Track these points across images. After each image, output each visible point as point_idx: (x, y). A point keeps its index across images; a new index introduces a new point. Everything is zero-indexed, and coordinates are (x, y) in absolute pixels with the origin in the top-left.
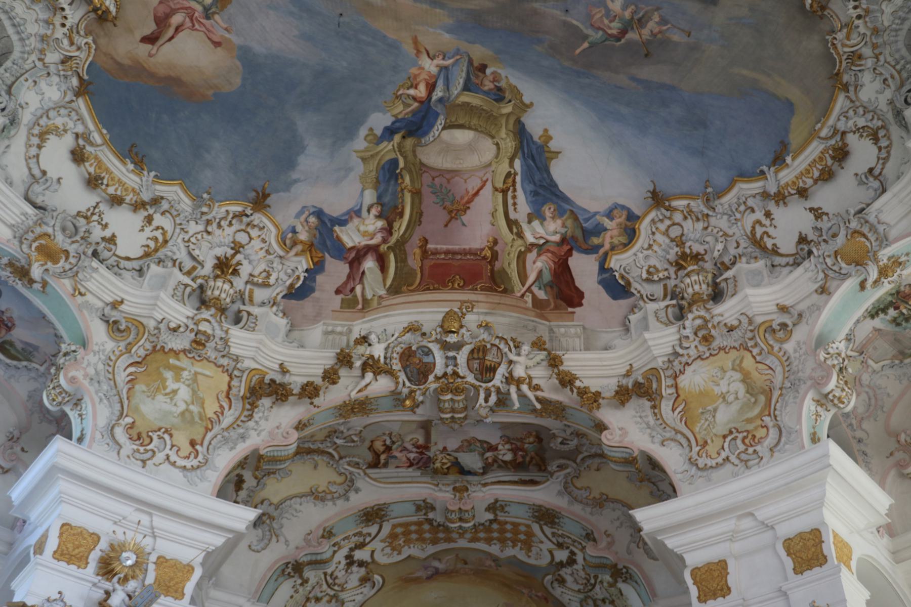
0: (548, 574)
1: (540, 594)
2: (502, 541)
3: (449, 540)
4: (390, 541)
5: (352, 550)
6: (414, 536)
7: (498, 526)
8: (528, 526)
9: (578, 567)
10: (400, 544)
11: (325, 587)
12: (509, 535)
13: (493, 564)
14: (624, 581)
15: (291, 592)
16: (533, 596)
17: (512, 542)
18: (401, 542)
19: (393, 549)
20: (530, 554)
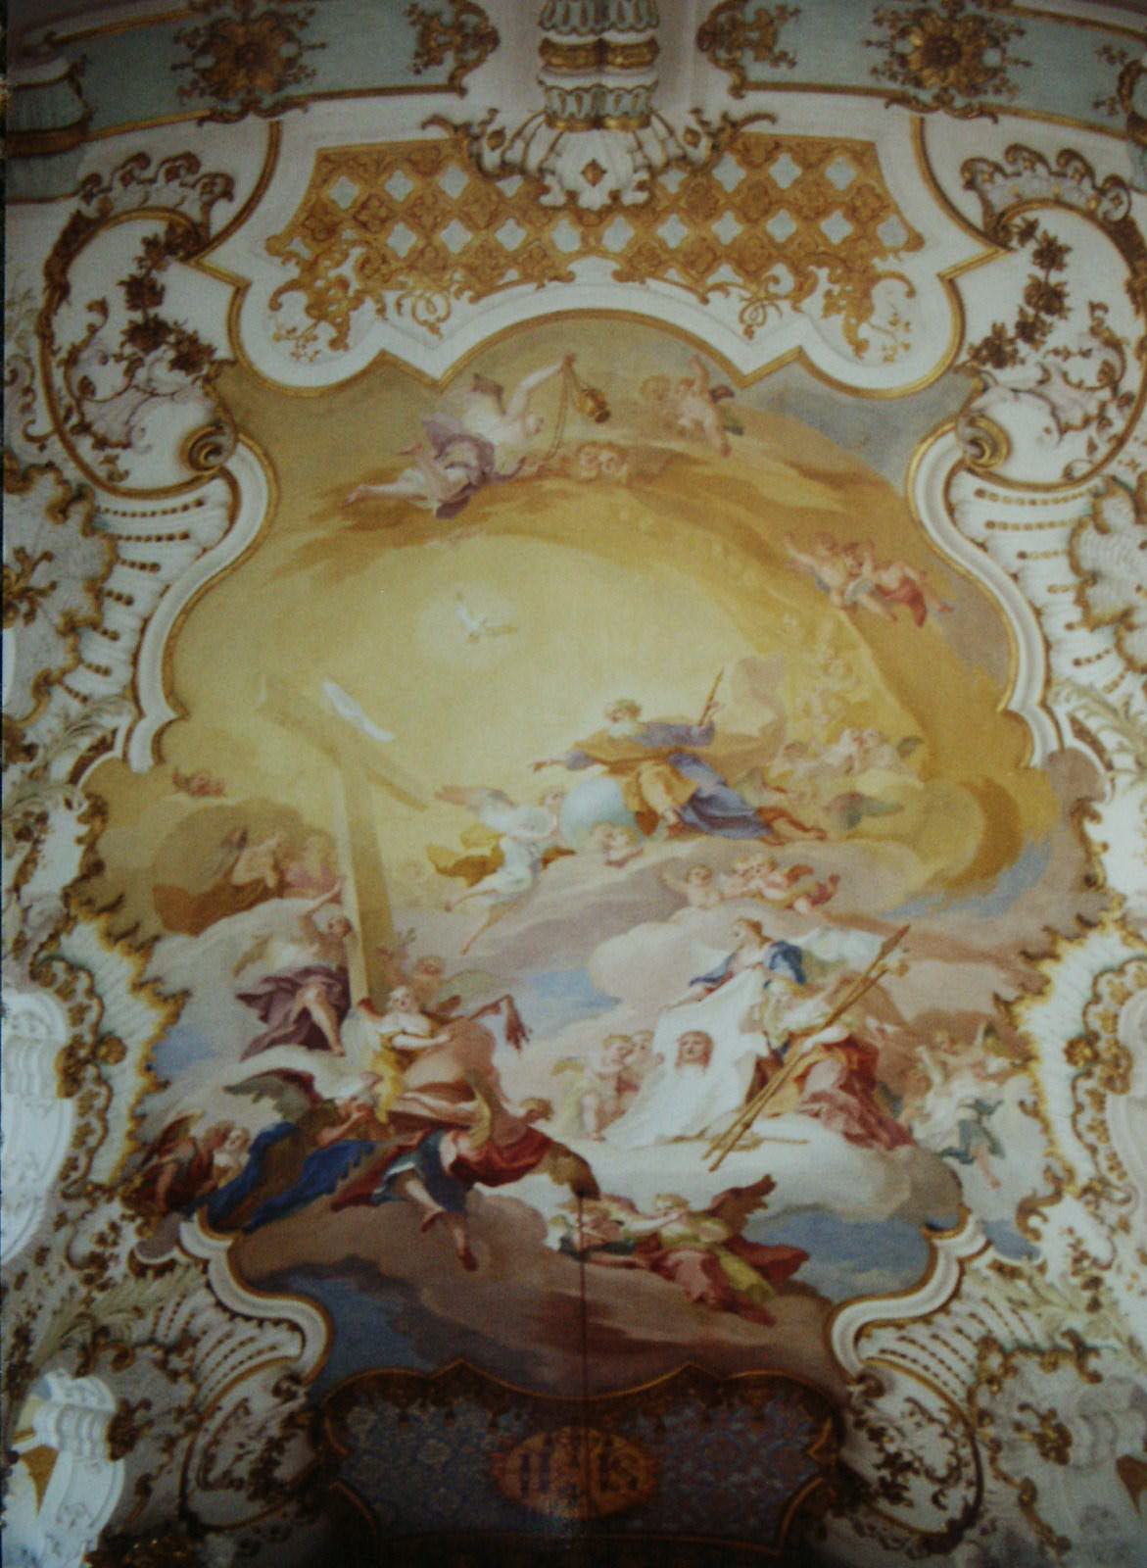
0: (935, 432)
1: (890, 578)
2: (752, 262)
3: (542, 267)
4: (306, 253)
5: (157, 251)
6: (402, 240)
7: (741, 174)
8: (864, 154)
9: (1067, 331)
10: (343, 284)
12: (781, 227)
13: (709, 418)
16: (864, 599)
17: (796, 269)
18: (347, 270)
19: (318, 309)
20: (864, 332)
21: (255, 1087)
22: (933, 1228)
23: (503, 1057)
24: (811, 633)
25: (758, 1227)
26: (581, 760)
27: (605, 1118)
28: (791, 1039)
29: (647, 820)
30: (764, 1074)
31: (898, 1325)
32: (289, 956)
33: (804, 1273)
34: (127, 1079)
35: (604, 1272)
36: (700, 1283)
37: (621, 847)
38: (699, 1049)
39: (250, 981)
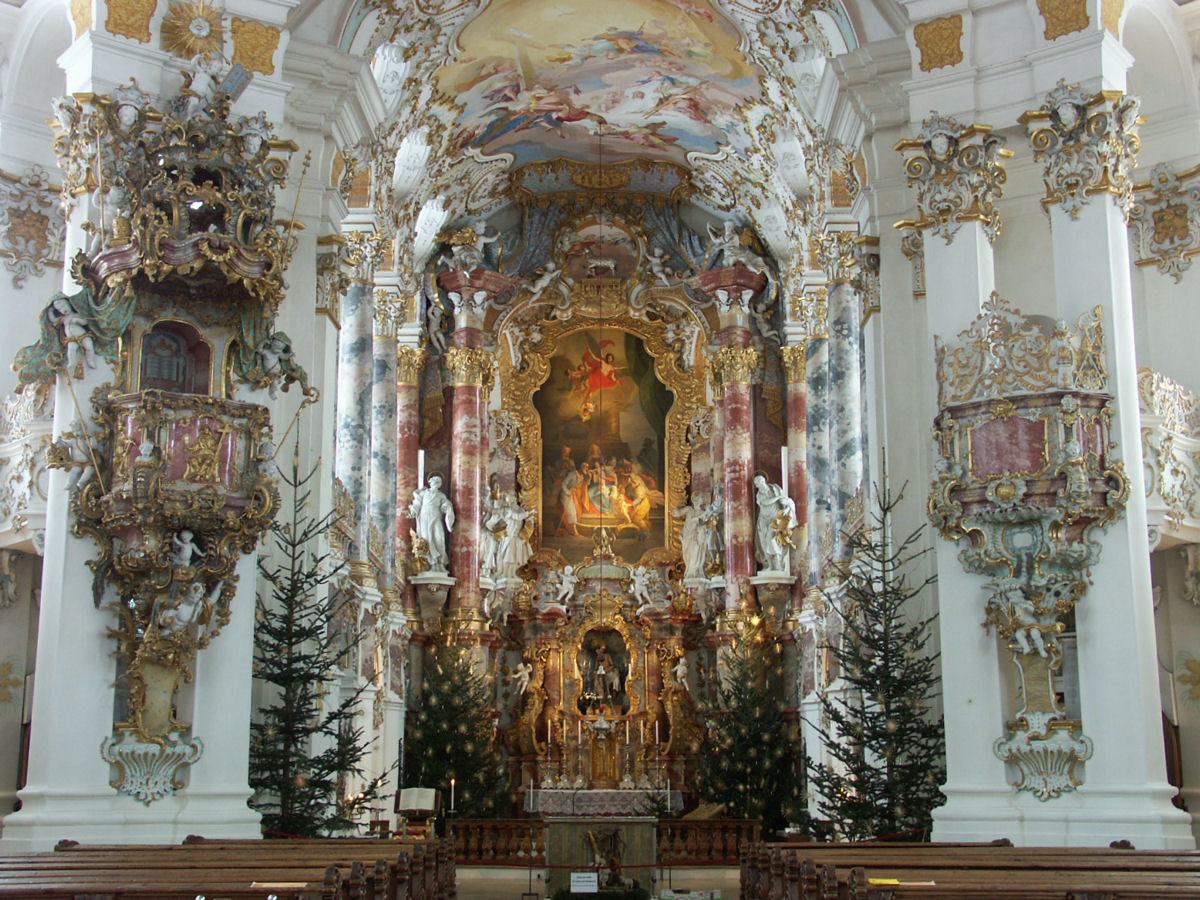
1: (702, 11)
11: (417, 11)
14: (820, 9)
15: (376, 24)
21: (490, 113)
22: (719, 144)
23: (573, 97)
24: (675, 17)
25: (660, 131)
26: (596, 38)
27: (608, 109)
28: (670, 95)
29: (621, 50)
30: (661, 102)
31: (708, 160)
32: (498, 85)
33: (676, 142)
34: (446, 135)
35: (608, 140)
36: (642, 141)
37: (611, 55)
38: (642, 96)
39: (486, 93)
